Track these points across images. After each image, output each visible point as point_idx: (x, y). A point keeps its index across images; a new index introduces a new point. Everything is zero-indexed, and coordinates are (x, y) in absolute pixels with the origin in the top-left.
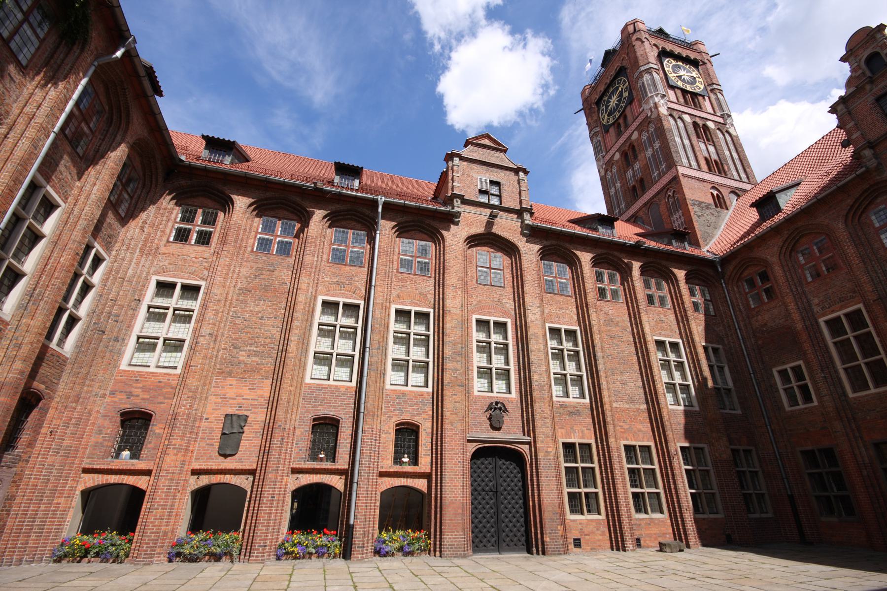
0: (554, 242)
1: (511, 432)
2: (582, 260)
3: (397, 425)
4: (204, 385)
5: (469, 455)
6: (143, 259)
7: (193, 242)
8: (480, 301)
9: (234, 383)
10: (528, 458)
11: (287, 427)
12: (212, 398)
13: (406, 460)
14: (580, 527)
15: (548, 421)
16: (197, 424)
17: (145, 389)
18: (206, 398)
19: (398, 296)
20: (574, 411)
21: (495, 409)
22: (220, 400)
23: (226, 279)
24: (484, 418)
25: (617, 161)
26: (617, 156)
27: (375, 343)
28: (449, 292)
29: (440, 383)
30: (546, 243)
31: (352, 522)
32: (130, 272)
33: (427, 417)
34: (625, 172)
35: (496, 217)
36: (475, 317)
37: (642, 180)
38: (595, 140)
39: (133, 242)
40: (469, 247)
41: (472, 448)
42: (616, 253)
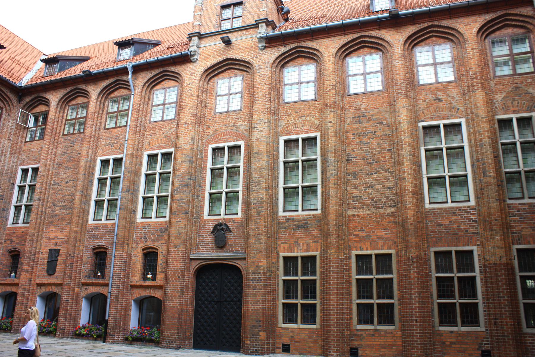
0: (293, 46)
4: (39, 232)
5: (192, 271)
6: (12, 158)
7: (37, 138)
8: (216, 130)
9: (54, 229)
11: (76, 255)
12: (44, 240)
13: (149, 276)
14: (291, 334)
15: (262, 237)
16: (37, 256)
17: (18, 238)
18: (41, 240)
19: (149, 143)
22: (47, 241)
23: (46, 160)
24: (210, 239)
31: (107, 318)
32: (6, 167)
33: (164, 242)
36: (211, 146)
39: (5, 149)
41: (195, 265)
42: (373, 33)
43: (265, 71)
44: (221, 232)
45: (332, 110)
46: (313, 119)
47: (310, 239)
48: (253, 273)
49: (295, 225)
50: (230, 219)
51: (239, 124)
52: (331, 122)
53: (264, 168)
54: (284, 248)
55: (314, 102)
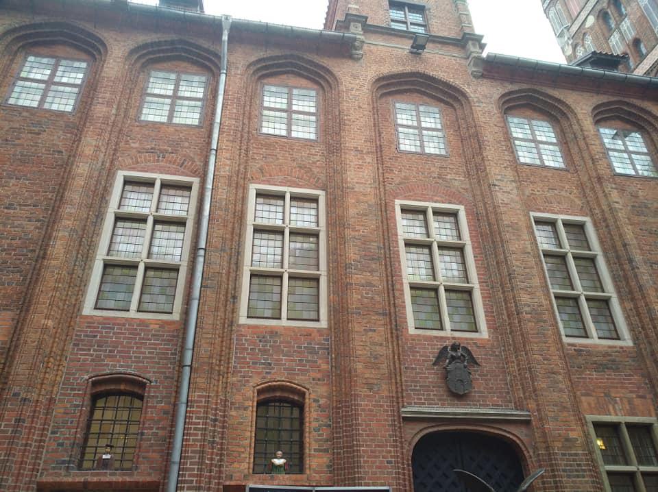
1: (486, 405)
2: (578, 110)
3: (260, 392)
5: (408, 450)
8: (406, 178)
10: (529, 453)
15: (560, 378)
19: (261, 170)
20: (606, 363)
21: (453, 358)
24: (431, 376)
25: (591, 28)
26: (591, 20)
27: (217, 242)
28: (351, 160)
29: (339, 311)
30: (510, 87)
34: (607, 39)
35: (423, 47)
36: (398, 203)
37: (637, 42)
38: (552, 11)
40: (383, 95)
41: (414, 434)
43: (490, 108)
44: (455, 363)
45: (614, 186)
46: (572, 196)
47: (631, 392)
48: (564, 455)
49: (595, 362)
50: (466, 339)
51: (449, 177)
52: (617, 203)
53: (529, 253)
54: (589, 404)
55: (565, 173)
